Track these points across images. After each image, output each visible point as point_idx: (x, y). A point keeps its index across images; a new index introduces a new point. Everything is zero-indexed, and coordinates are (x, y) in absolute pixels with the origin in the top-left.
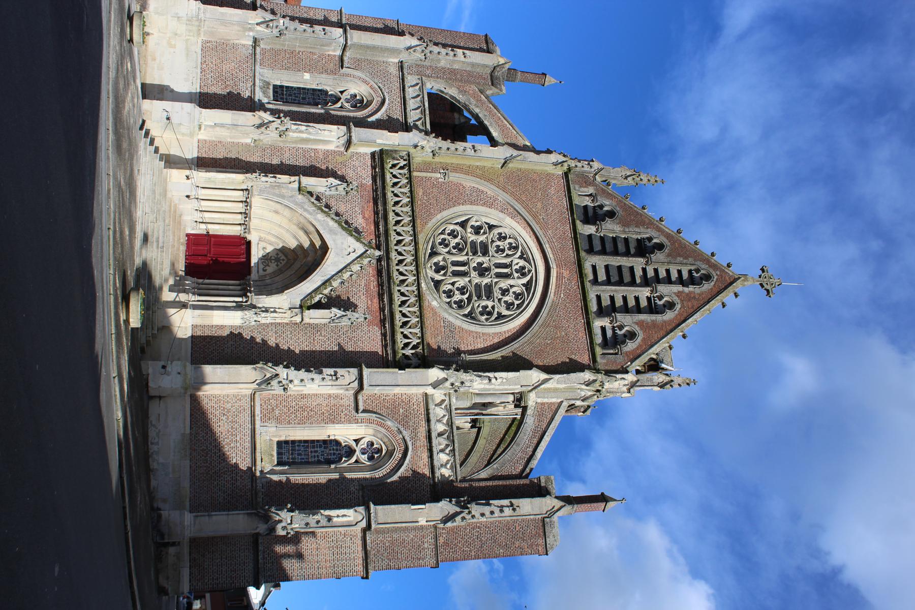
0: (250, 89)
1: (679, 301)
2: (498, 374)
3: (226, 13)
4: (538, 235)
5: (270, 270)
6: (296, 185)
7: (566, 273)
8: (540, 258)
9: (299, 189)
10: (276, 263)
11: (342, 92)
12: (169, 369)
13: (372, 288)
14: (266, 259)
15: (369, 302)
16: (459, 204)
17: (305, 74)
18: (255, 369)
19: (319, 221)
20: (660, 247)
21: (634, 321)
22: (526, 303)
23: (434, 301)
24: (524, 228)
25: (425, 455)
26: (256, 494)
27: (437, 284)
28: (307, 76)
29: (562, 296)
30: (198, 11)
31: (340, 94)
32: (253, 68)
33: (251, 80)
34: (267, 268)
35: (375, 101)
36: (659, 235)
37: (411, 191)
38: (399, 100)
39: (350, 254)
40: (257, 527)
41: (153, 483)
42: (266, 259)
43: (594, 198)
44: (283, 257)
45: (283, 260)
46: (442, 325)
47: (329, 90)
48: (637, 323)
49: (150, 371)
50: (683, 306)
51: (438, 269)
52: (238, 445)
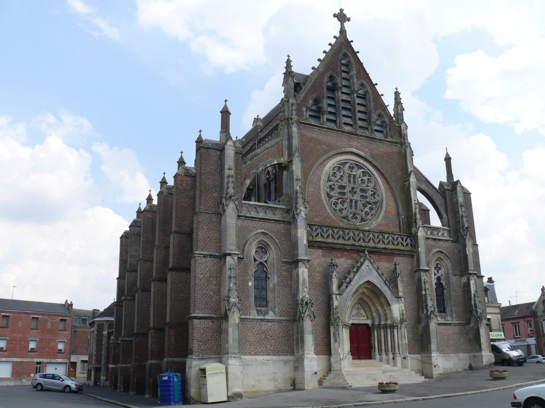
0: (266, 323)
1: (361, 80)
2: (413, 200)
3: (233, 339)
4: (336, 153)
5: (364, 313)
6: (338, 296)
7: (355, 144)
8: (345, 156)
9: (340, 294)
10: (360, 310)
11: (255, 260)
12: (435, 364)
13: (376, 258)
14: (358, 315)
15: (383, 260)
16: (321, 197)
17: (249, 285)
18: (430, 322)
19: (355, 284)
20: (331, 78)
21: (374, 112)
22: (369, 171)
23: (373, 225)
24: (331, 160)
25: (441, 243)
26: (461, 324)
27: (363, 220)
28: (250, 284)
29: (367, 150)
30: (236, 359)
31: (257, 262)
32: (251, 320)
33: (259, 322)
34: (363, 315)
35: (264, 239)
36: (326, 75)
37: (326, 227)
38: (261, 223)
39: (369, 269)
40: (484, 323)
41: (460, 370)
42: (358, 315)
43: (308, 109)
44: (357, 306)
45: (358, 305)
46: (384, 222)
47: (255, 270)
48: (375, 111)
49: (437, 373)
50: (364, 79)
51: (355, 216)
52: (444, 331)
